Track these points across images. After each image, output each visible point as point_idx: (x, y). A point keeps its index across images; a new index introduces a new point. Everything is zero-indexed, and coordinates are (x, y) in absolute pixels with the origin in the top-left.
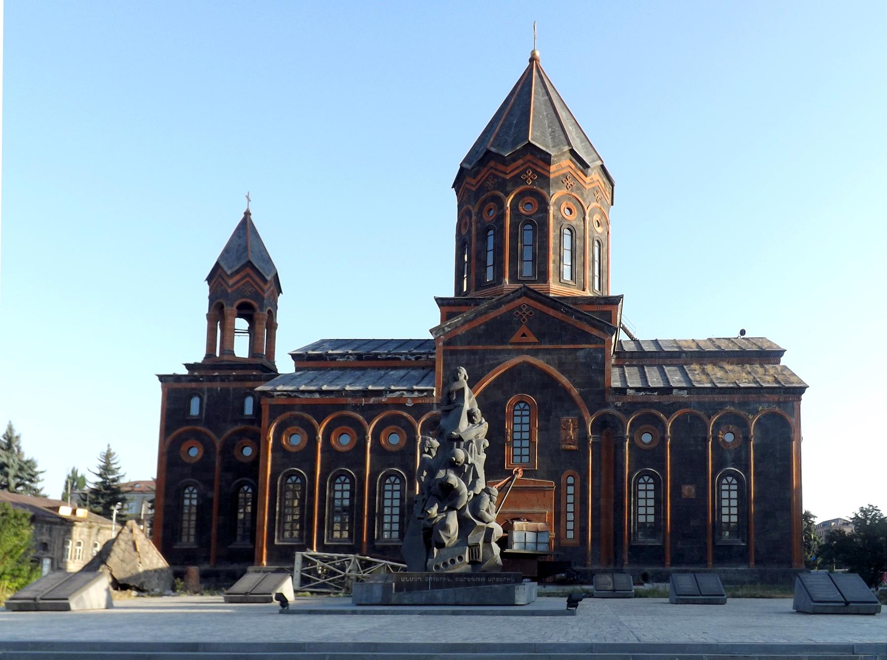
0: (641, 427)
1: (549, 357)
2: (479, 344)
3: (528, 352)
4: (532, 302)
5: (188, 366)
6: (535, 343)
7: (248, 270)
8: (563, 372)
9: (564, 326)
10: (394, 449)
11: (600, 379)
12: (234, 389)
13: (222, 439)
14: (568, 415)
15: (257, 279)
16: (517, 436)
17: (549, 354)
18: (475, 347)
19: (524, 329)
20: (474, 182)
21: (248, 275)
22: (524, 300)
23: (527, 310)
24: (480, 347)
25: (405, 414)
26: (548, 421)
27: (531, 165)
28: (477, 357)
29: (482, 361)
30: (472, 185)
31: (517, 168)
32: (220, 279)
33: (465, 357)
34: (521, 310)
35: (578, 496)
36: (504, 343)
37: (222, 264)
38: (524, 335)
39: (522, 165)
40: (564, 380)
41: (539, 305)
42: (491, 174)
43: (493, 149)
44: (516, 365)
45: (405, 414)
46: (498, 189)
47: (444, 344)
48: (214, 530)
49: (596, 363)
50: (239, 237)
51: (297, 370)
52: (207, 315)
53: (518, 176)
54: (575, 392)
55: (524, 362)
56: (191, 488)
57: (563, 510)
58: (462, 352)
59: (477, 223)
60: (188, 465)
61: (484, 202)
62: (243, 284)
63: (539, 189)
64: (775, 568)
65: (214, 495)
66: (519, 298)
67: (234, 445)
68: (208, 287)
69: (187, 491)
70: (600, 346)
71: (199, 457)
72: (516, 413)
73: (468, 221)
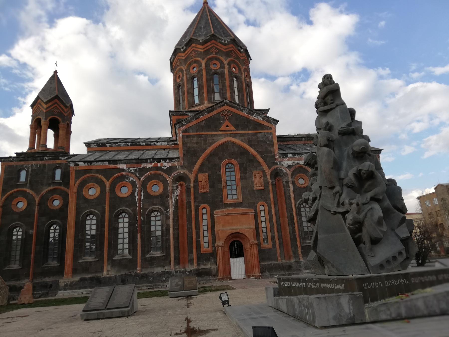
0: (298, 175)
1: (242, 138)
2: (202, 131)
3: (230, 135)
4: (230, 108)
5: (16, 153)
6: (234, 130)
7: (57, 100)
8: (251, 146)
10: (156, 194)
11: (271, 149)
12: (49, 165)
13: (40, 196)
14: (257, 169)
15: (62, 106)
16: (228, 183)
17: (243, 136)
18: (201, 133)
19: (227, 123)
20: (183, 55)
21: (56, 103)
22: (226, 107)
23: (228, 112)
24: (204, 133)
25: (162, 173)
26: (246, 173)
27: (215, 45)
28: (202, 139)
29: (205, 141)
30: (183, 56)
31: (208, 46)
32: (39, 105)
33: (195, 139)
34: (225, 113)
35: (267, 217)
36: (216, 131)
37: (41, 97)
38: (227, 126)
39: (210, 45)
40: (252, 151)
42: (193, 50)
43: (194, 37)
44: (225, 142)
45: (162, 173)
46: (198, 57)
47: (182, 132)
48: (32, 256)
49: (269, 140)
50: (51, 83)
51: (89, 152)
52: (30, 125)
53: (208, 50)
54: (259, 157)
55: (229, 141)
56: (18, 229)
57: (260, 226)
58: (193, 136)
59: (187, 74)
61: (190, 64)
63: (220, 57)
65: (33, 232)
66: (223, 105)
67: (48, 199)
68: (31, 110)
69: (15, 230)
70: (269, 131)
71: (24, 208)
72: (227, 170)
73: (181, 75)
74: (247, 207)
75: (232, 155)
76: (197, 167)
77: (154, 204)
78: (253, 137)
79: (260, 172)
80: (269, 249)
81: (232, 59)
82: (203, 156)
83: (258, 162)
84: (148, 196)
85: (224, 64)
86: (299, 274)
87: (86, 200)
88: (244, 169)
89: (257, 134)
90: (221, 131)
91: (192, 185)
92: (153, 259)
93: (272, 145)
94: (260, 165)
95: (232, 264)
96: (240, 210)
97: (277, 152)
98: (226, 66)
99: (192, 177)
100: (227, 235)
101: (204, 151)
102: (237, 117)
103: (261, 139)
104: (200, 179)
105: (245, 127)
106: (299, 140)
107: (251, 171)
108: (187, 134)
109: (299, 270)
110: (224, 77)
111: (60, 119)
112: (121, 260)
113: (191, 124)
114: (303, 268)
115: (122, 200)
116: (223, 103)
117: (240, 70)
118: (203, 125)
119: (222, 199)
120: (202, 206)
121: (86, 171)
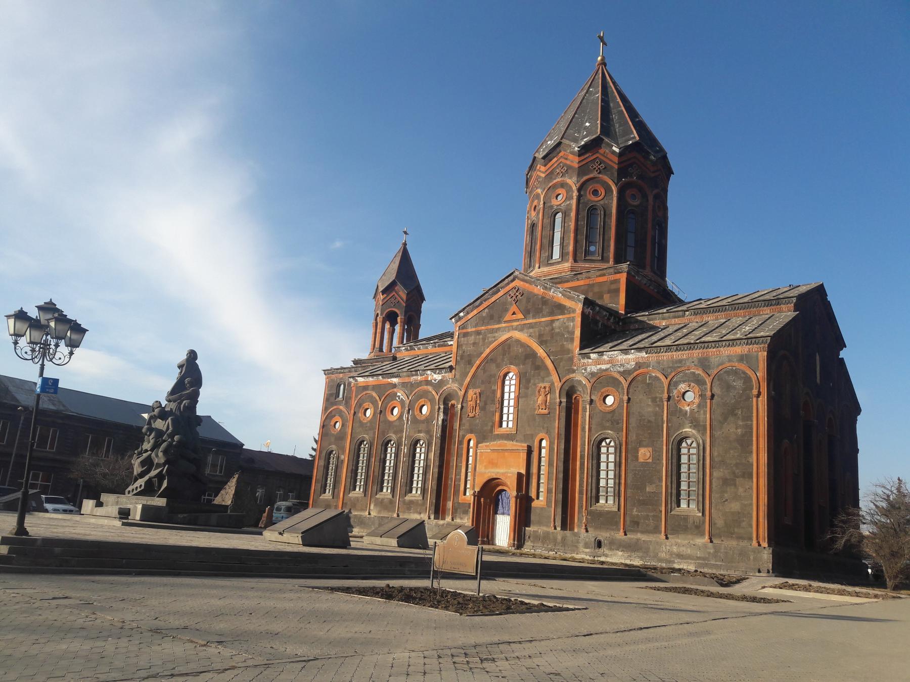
1: (531, 330)
8: (542, 343)
9: (544, 301)
10: (423, 418)
11: (570, 346)
14: (543, 382)
25: (430, 388)
26: (527, 388)
29: (484, 339)
36: (499, 322)
38: (514, 313)
40: (541, 352)
41: (527, 285)
44: (507, 340)
49: (568, 332)
54: (548, 363)
60: (333, 435)
61: (533, 201)
64: (733, 543)
66: (513, 280)
70: (572, 315)
74: (521, 442)
76: (468, 379)
77: (420, 432)
78: (547, 329)
79: (547, 385)
80: (542, 509)
81: (591, 176)
82: (478, 362)
83: (546, 368)
84: (415, 421)
85: (573, 192)
86: (573, 551)
87: (361, 424)
88: (524, 382)
89: (553, 321)
90: (505, 322)
91: (459, 406)
92: (411, 502)
93: (572, 340)
94: (548, 374)
96: (509, 444)
97: (577, 351)
98: (575, 194)
99: (461, 393)
100: (485, 480)
102: (530, 297)
103: (557, 330)
104: (470, 399)
105: (538, 312)
106: (679, 317)
107: (535, 384)
108: (465, 331)
109: (575, 548)
110: (569, 215)
112: (383, 500)
113: (470, 316)
114: (581, 545)
115: (391, 423)
116: (512, 277)
118: (484, 314)
119: (493, 426)
120: (468, 436)
121: (365, 388)
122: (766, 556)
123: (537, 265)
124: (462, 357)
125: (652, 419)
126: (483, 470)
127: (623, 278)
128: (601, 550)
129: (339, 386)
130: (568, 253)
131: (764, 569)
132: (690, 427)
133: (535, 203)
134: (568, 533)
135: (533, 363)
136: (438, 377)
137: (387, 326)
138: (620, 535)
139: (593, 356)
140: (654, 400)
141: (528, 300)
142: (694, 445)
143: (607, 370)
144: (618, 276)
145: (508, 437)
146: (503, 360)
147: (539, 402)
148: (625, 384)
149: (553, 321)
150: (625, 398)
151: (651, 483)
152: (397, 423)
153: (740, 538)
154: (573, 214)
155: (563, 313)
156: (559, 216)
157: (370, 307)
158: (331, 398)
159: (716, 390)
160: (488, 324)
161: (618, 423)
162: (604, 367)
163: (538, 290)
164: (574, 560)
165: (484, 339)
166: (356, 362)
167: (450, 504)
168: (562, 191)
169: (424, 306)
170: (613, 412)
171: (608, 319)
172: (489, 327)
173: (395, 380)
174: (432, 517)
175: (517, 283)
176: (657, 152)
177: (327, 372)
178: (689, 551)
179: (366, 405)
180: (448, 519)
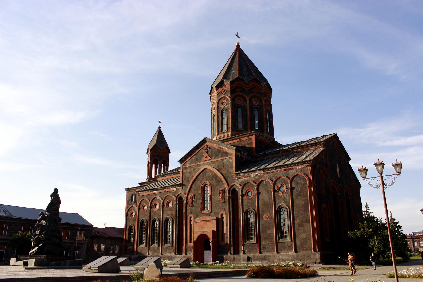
8: (218, 171)
11: (231, 171)
14: (221, 188)
17: (215, 163)
36: (200, 162)
38: (206, 157)
41: (211, 144)
55: (206, 168)
62: (159, 152)
63: (227, 97)
70: (231, 156)
74: (213, 216)
75: (208, 178)
77: (168, 215)
83: (222, 181)
89: (223, 159)
93: (232, 167)
94: (223, 184)
95: (205, 254)
96: (208, 218)
101: (193, 177)
105: (217, 156)
108: (185, 167)
111: (158, 159)
117: (245, 100)
121: (143, 196)
122: (318, 256)
123: (216, 134)
124: (185, 179)
125: (268, 200)
126: (197, 231)
127: (253, 137)
128: (250, 262)
129: (132, 196)
130: (229, 128)
131: (318, 262)
132: (283, 203)
133: (214, 106)
134: (236, 256)
135: (216, 179)
136: (174, 189)
137: (153, 166)
138: (258, 254)
139: (241, 174)
140: (268, 192)
141: (212, 150)
142: (286, 210)
143: (248, 180)
144: (251, 137)
145: (208, 214)
146: (203, 179)
147: (220, 197)
148: (255, 186)
149: (223, 159)
150: (256, 192)
151: (269, 229)
152: (158, 212)
153: (307, 250)
154: (230, 111)
155: (227, 156)
156: (225, 111)
157: (146, 158)
158: (130, 201)
159: (293, 186)
160: (195, 163)
161: (254, 204)
162: (246, 179)
163: (216, 146)
164: (239, 267)
165: (194, 170)
166: (140, 184)
167: (184, 248)
168: (225, 101)
169: (170, 155)
170: (252, 198)
171: (248, 156)
172: (196, 164)
173: (156, 192)
174: (177, 254)
175: (207, 144)
176: (264, 82)
177: (127, 190)
178: (286, 258)
179: (143, 204)
180: (184, 254)
